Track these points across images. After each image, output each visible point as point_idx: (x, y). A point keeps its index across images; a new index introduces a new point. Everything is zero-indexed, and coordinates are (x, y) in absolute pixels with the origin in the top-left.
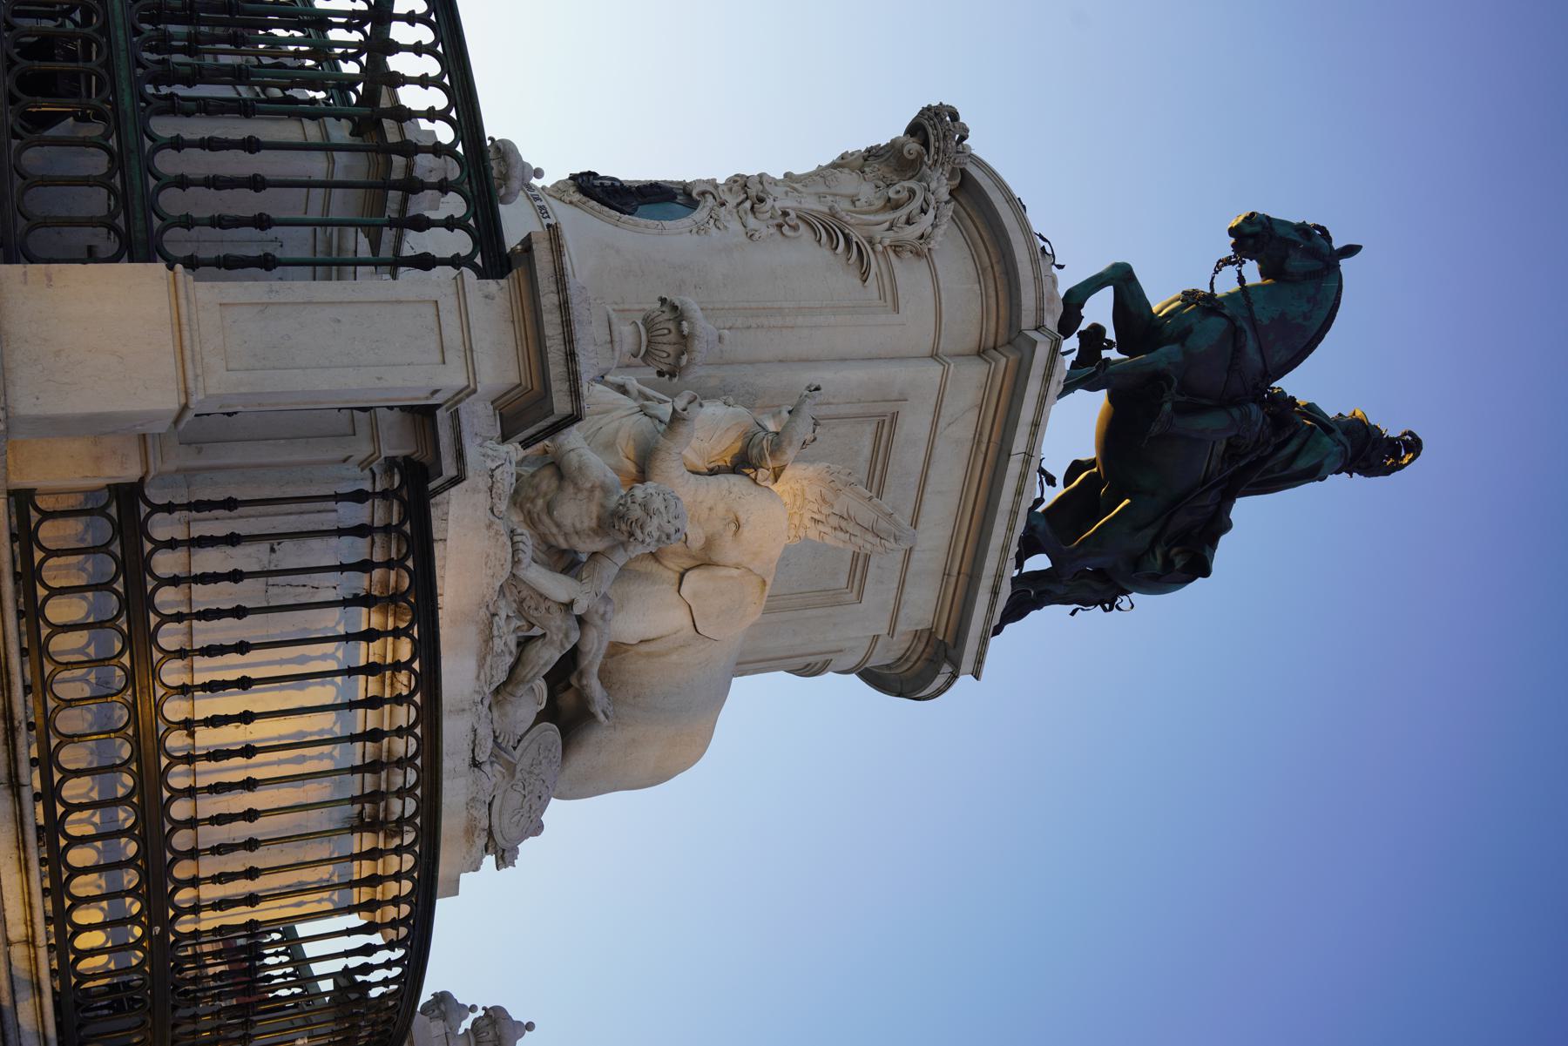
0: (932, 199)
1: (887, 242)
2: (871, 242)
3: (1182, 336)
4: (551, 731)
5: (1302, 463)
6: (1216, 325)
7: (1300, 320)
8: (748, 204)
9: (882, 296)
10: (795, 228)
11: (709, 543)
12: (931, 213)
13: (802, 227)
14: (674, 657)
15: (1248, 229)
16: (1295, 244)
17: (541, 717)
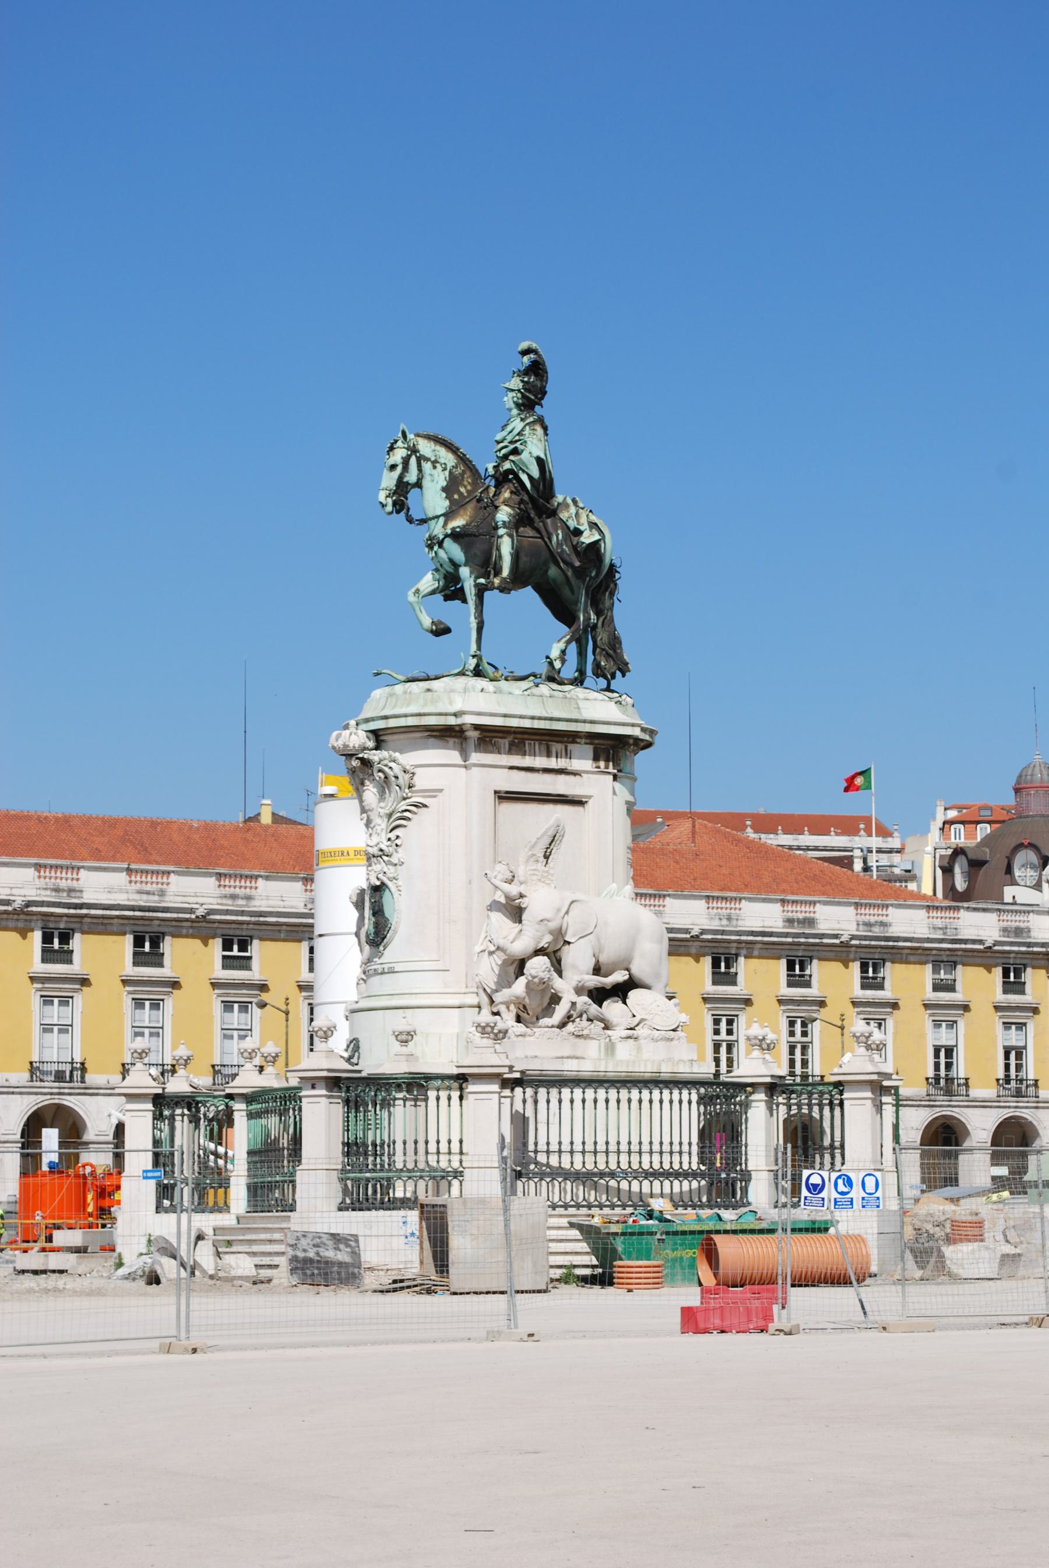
0: (385, 762)
1: (407, 790)
2: (404, 799)
3: (456, 566)
4: (633, 995)
5: (535, 473)
6: (448, 543)
7: (447, 473)
8: (385, 858)
9: (435, 797)
10: (398, 837)
11: (551, 933)
12: (392, 764)
13: (397, 832)
14: (602, 941)
15: (389, 508)
16: (400, 478)
17: (625, 1003)
